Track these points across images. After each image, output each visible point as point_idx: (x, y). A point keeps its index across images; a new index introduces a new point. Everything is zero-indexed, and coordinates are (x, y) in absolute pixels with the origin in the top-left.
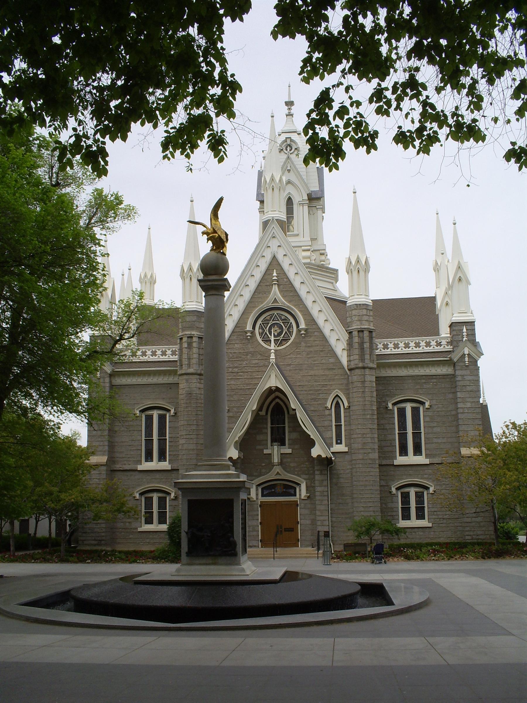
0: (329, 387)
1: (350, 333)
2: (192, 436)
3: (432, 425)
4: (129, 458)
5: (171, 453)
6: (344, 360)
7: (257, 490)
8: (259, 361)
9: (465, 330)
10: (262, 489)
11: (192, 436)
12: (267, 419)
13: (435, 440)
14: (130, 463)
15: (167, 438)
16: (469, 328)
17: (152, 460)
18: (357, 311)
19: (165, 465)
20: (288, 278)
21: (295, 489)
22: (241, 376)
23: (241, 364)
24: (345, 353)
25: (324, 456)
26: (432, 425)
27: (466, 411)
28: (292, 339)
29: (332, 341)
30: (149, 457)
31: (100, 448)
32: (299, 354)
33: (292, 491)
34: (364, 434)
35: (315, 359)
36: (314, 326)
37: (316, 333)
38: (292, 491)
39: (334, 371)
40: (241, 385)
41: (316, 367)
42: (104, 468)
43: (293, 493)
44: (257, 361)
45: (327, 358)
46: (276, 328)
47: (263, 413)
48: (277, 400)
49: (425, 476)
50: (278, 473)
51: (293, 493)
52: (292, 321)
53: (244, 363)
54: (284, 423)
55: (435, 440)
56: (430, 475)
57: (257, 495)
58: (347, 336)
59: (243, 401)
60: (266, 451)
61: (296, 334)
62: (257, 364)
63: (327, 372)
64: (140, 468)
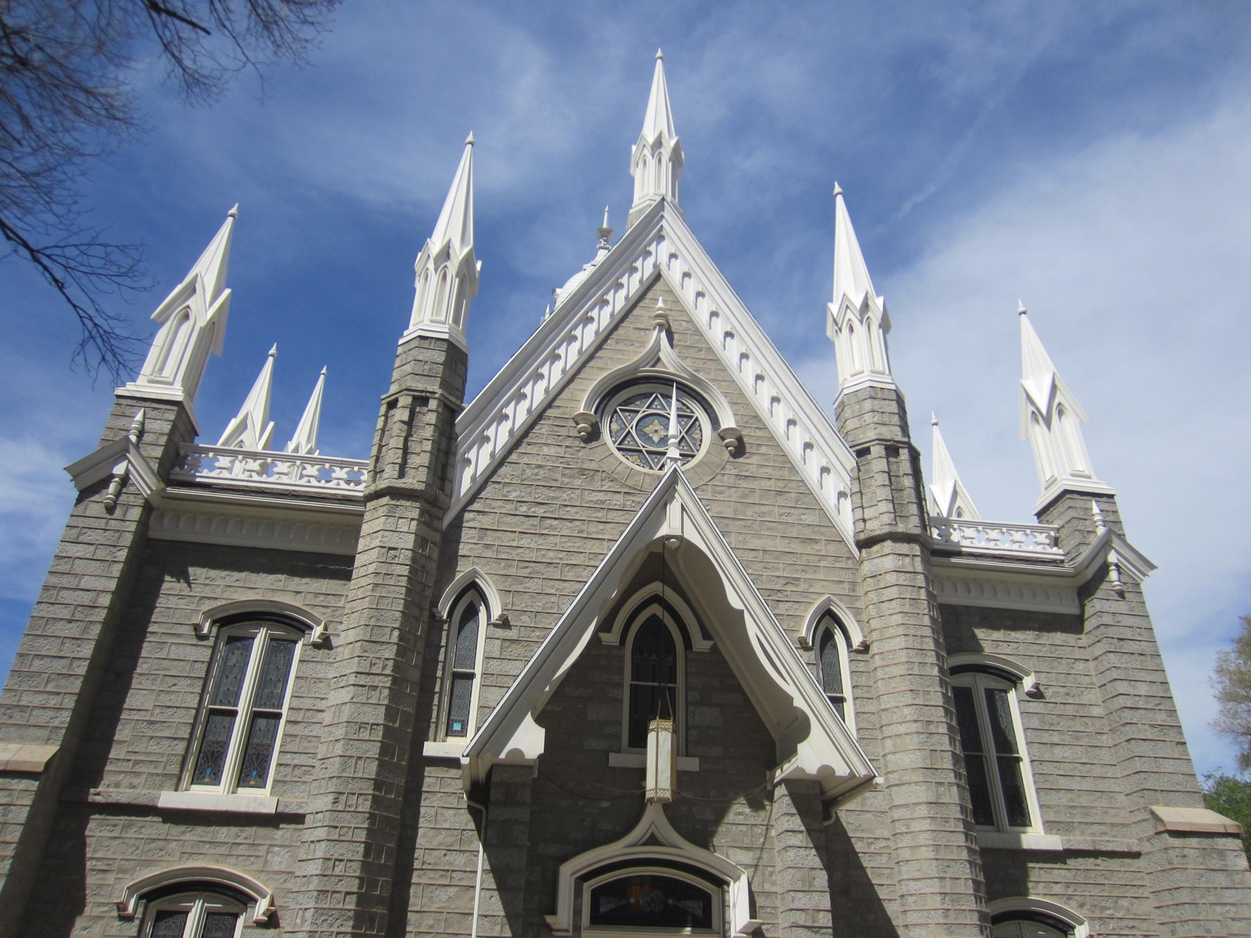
0: (803, 587)
1: (862, 452)
2: (377, 681)
3: (1046, 737)
4: (137, 762)
5: (287, 758)
6: (846, 521)
7: (578, 894)
8: (609, 496)
9: (1096, 510)
10: (596, 894)
11: (377, 681)
12: (621, 659)
13: (1063, 783)
14: (136, 781)
15: (284, 710)
16: (1105, 506)
17: (216, 780)
18: (876, 402)
19: (258, 799)
20: (691, 321)
21: (706, 898)
22: (551, 527)
23: (553, 498)
24: (847, 504)
25: (841, 770)
26: (1046, 737)
27: (1141, 704)
28: (700, 455)
29: (811, 471)
30: (207, 766)
31: (42, 717)
32: (721, 493)
33: (695, 907)
34: (929, 722)
35: (765, 509)
36: (759, 433)
37: (763, 450)
38: (695, 907)
39: (817, 547)
40: (551, 554)
41: (769, 529)
42: (34, 785)
43: (699, 913)
44: (601, 496)
45: (793, 511)
46: (656, 425)
47: (611, 638)
48: (655, 609)
49: (1057, 889)
50: (653, 840)
51: (699, 913)
52: (700, 413)
53: (565, 496)
54: (673, 679)
55: (1063, 783)
56: (1067, 885)
57: (577, 912)
58: (850, 461)
59: (553, 599)
60: (615, 760)
61: (712, 444)
62: (603, 502)
63: (796, 547)
64: (169, 799)
